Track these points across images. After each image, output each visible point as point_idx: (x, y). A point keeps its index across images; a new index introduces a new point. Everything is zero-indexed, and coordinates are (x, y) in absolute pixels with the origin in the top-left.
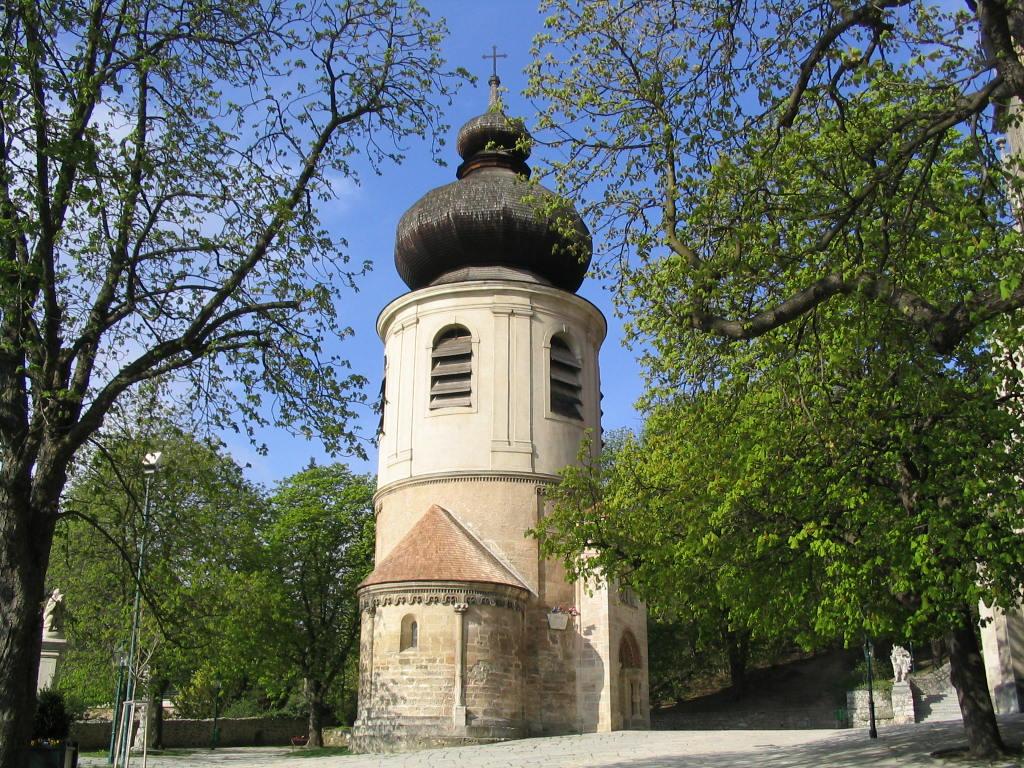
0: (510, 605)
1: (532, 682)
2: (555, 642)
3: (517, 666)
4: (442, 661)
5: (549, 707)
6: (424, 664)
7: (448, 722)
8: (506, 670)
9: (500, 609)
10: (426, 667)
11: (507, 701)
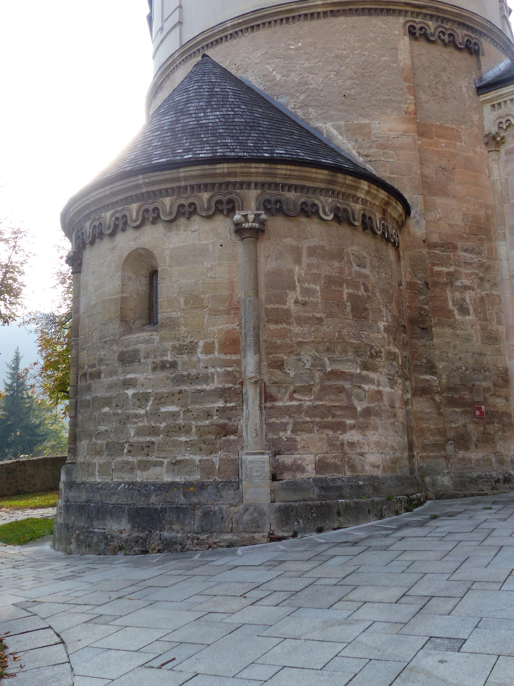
0: (367, 225)
1: (423, 391)
2: (464, 311)
3: (392, 357)
4: (208, 349)
5: (462, 441)
6: (169, 358)
7: (229, 494)
8: (365, 366)
9: (344, 230)
10: (173, 365)
11: (373, 436)
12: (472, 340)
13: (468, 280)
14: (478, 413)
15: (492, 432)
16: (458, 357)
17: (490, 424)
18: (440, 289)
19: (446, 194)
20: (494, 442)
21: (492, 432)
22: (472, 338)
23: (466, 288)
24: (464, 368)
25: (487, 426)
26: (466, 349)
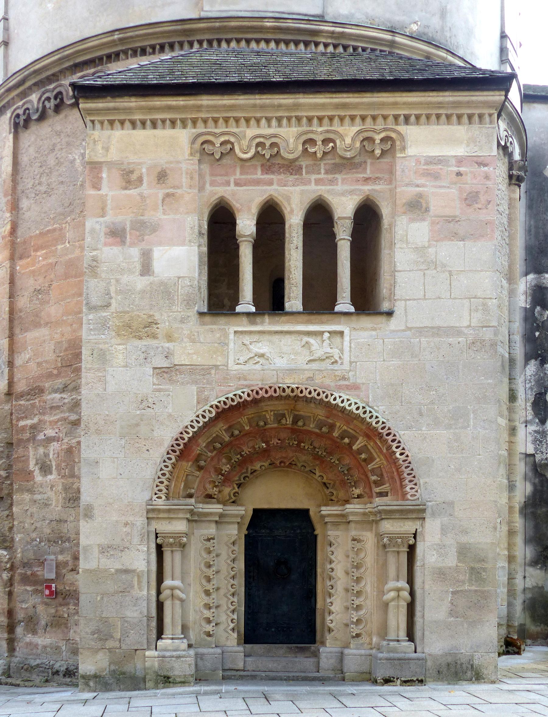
12: (51, 504)
13: (53, 429)
14: (47, 592)
15: (66, 616)
16: (33, 527)
17: (63, 605)
18: (23, 448)
19: (37, 325)
20: (67, 628)
21: (66, 616)
22: (50, 502)
23: (49, 440)
24: (38, 540)
25: (60, 608)
26: (44, 516)
